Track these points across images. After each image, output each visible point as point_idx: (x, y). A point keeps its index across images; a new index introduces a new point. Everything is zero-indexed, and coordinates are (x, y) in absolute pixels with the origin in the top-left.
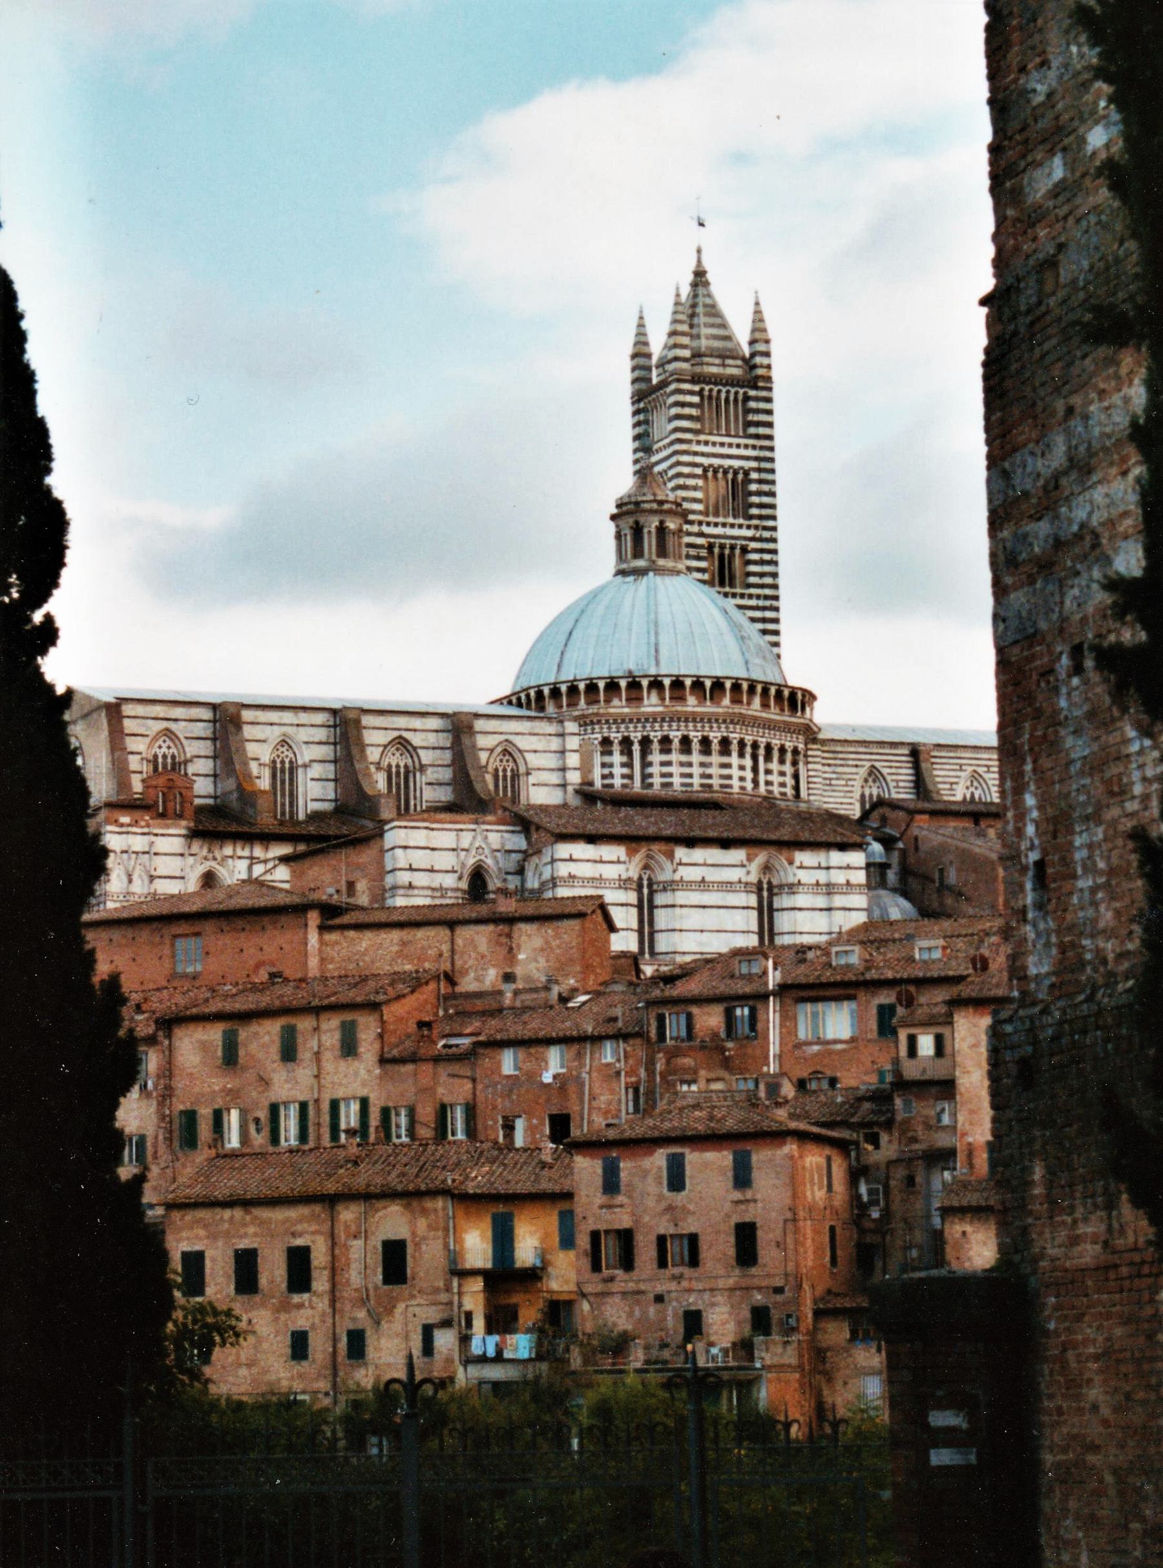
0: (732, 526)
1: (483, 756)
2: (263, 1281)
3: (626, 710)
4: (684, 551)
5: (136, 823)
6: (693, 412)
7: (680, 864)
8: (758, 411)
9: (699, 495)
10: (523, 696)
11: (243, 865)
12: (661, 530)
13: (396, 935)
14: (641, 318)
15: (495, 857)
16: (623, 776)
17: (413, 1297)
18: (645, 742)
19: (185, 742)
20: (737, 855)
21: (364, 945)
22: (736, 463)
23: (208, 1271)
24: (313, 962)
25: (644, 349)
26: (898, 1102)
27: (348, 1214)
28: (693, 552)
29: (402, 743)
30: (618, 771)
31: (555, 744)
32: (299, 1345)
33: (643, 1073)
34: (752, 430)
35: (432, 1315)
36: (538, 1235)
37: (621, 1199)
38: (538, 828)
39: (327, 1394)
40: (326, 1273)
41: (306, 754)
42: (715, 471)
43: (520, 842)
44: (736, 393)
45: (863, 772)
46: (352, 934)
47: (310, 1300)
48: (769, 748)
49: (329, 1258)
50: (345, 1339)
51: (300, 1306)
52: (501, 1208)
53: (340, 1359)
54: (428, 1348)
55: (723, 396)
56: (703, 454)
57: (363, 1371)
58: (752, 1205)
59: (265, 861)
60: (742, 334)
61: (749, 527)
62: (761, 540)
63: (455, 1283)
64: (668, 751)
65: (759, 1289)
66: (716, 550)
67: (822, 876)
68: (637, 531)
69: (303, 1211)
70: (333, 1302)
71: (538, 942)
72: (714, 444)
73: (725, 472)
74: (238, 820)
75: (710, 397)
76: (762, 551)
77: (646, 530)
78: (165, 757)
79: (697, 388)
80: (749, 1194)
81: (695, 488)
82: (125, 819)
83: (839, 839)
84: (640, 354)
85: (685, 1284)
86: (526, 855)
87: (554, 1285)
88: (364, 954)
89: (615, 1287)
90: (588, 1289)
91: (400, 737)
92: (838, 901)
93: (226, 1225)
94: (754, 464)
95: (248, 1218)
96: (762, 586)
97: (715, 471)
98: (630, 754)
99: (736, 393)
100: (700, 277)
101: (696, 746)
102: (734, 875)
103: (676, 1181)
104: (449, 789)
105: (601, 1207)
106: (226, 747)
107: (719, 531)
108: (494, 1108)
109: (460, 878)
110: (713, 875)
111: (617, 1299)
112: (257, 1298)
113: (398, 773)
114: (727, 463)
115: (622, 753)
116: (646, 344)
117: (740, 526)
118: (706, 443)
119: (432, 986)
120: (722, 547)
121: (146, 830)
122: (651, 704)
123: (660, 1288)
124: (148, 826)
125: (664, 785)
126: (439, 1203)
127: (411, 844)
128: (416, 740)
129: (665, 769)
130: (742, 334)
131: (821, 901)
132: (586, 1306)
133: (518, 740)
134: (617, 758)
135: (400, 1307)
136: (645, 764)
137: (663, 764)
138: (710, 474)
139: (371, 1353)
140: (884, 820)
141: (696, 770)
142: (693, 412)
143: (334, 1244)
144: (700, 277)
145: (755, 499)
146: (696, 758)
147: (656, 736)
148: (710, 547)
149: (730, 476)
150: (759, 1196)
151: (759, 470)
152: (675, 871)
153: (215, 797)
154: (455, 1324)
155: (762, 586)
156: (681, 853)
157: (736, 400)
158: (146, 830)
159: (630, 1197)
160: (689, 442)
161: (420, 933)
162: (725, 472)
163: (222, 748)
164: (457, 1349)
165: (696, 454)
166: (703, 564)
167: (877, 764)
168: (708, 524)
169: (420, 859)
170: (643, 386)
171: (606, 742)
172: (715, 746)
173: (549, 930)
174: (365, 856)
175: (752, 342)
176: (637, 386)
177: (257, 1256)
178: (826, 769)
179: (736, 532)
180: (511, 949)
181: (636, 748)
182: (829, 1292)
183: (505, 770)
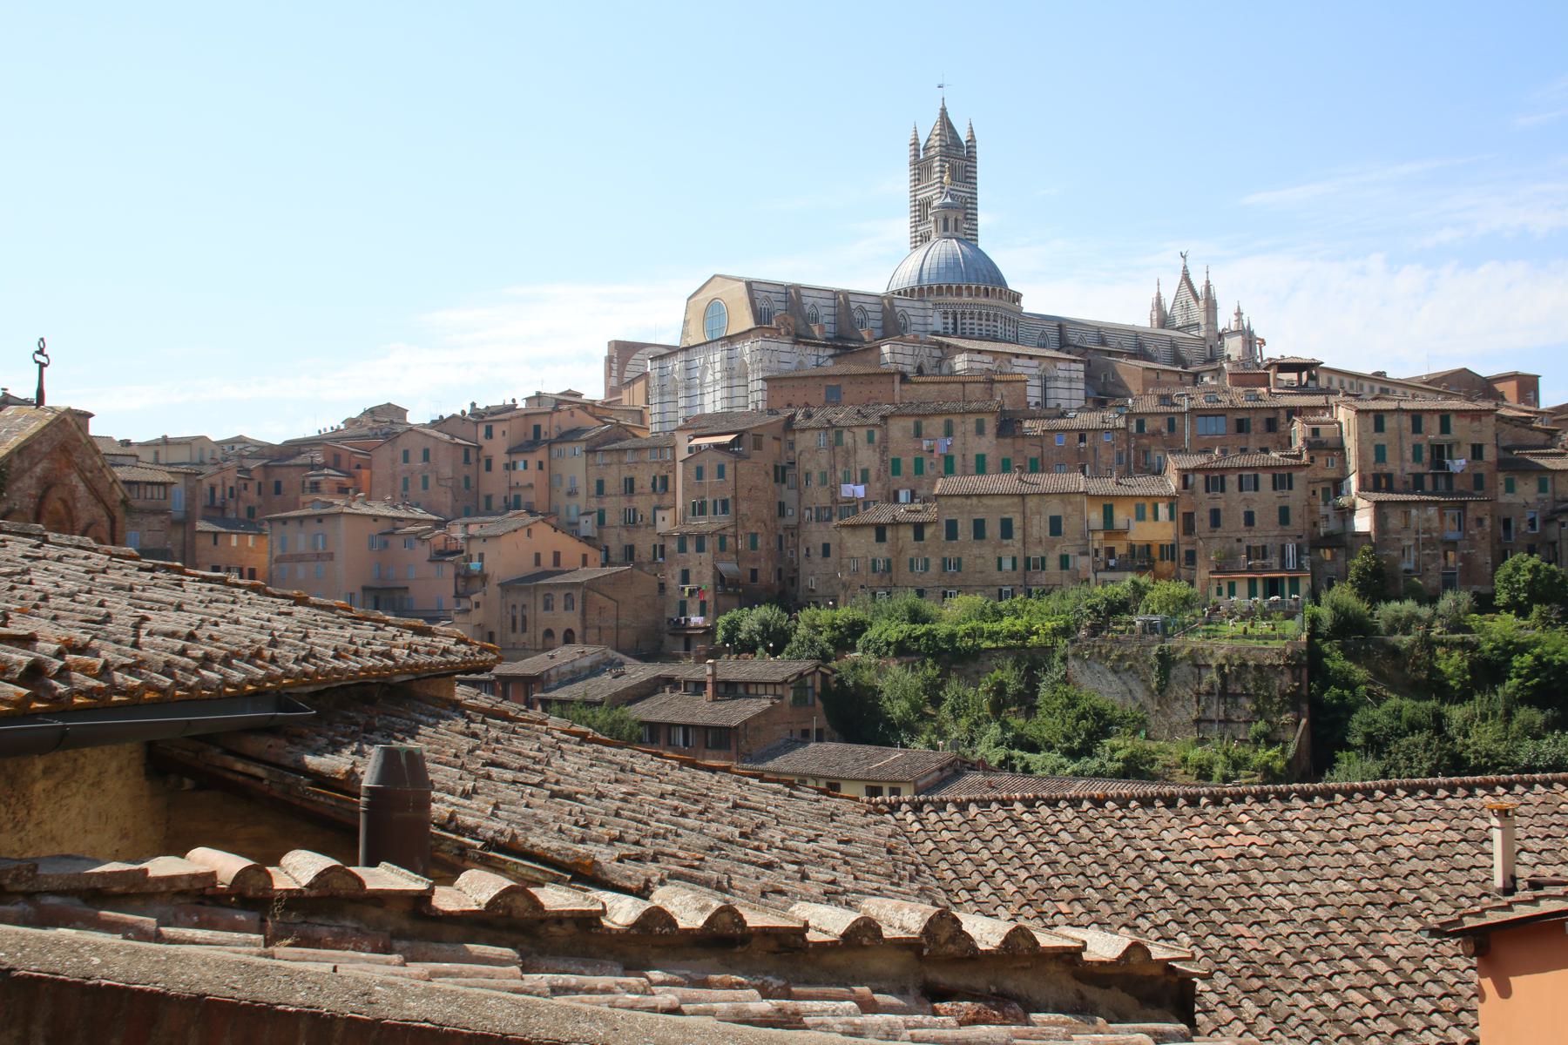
2: (988, 534)
13: (936, 387)
18: (963, 313)
20: (1035, 363)
24: (897, 399)
29: (861, 309)
31: (922, 313)
33: (1125, 446)
40: (1020, 531)
41: (823, 311)
43: (937, 353)
51: (1007, 545)
60: (964, 137)
67: (1067, 374)
68: (946, 220)
69: (1009, 501)
70: (1024, 543)
84: (916, 143)
92: (1074, 385)
100: (944, 112)
101: (984, 317)
102: (1034, 371)
112: (985, 541)
122: (965, 299)
123: (1239, 536)
126: (1078, 498)
128: (867, 307)
131: (1066, 385)
134: (950, 321)
135: (1058, 546)
141: (983, 327)
144: (944, 112)
146: (984, 322)
156: (1014, 360)
161: (948, 387)
171: (946, 313)
172: (992, 318)
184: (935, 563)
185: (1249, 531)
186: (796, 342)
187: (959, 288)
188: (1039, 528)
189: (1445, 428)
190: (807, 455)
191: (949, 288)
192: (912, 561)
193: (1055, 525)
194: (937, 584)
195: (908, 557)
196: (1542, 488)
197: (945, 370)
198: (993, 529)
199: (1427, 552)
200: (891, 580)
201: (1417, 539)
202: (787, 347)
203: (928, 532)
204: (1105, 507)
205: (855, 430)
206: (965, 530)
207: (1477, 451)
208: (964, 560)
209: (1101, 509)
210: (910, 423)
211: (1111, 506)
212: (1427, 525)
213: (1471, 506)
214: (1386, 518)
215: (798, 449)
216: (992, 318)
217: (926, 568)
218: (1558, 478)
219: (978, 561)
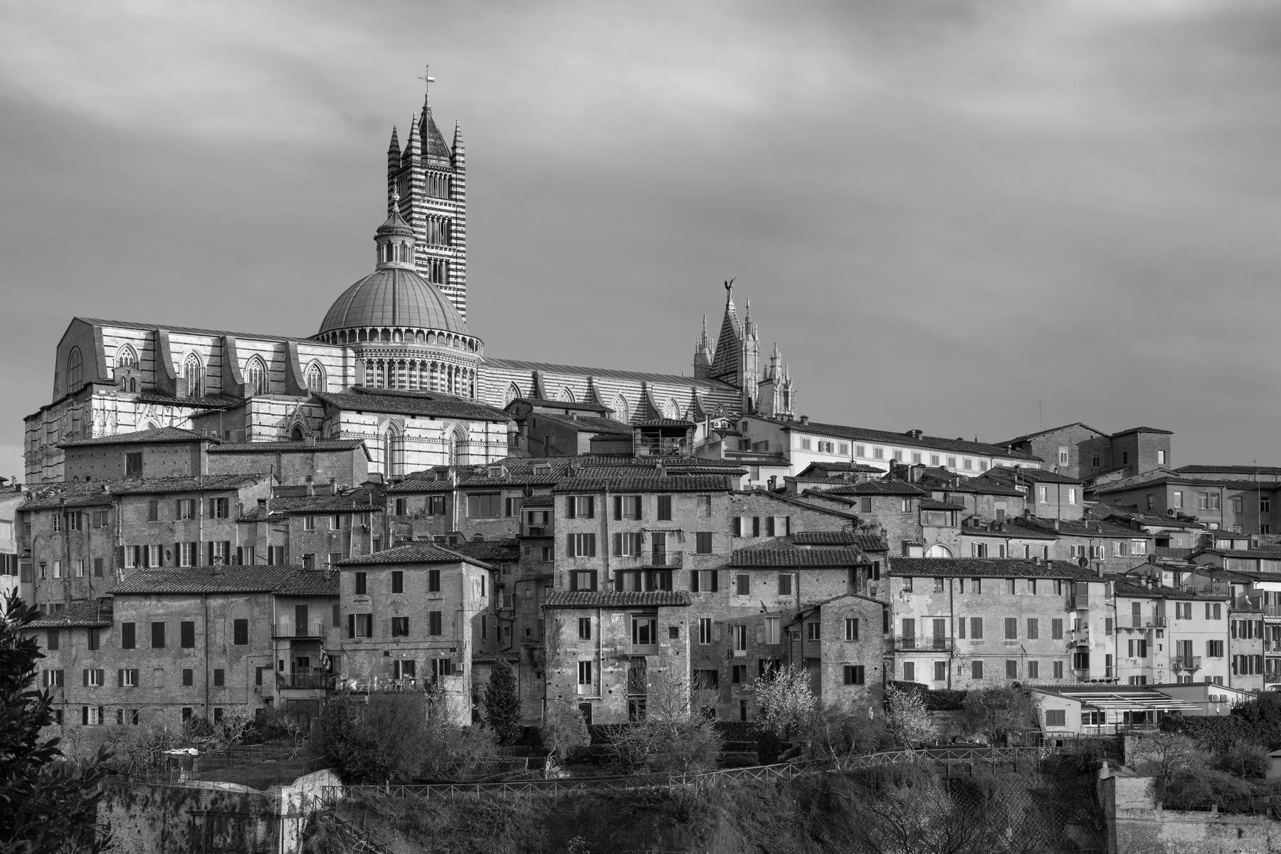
0: (441, 249)
1: (302, 367)
2: (167, 641)
3: (381, 345)
4: (415, 261)
5: (109, 394)
6: (422, 184)
7: (407, 427)
8: (456, 186)
9: (424, 230)
10: (325, 335)
11: (167, 420)
12: (404, 246)
14: (395, 132)
15: (307, 421)
16: (378, 381)
17: (251, 651)
19: (137, 351)
20: (438, 423)
21: (232, 462)
22: (444, 214)
23: (137, 633)
25: (396, 149)
26: (522, 548)
27: (215, 603)
28: (419, 262)
30: (376, 378)
32: (188, 678)
34: (454, 196)
35: (262, 662)
36: (321, 619)
37: (367, 597)
38: (331, 405)
39: (203, 705)
40: (203, 637)
42: (433, 218)
43: (318, 412)
44: (445, 175)
45: (508, 385)
46: (226, 456)
47: (194, 652)
48: (457, 370)
49: (205, 629)
50: (213, 674)
51: (189, 655)
52: (301, 603)
53: (210, 686)
54: (259, 680)
55: (438, 176)
56: (426, 208)
57: (223, 692)
58: (440, 601)
59: (180, 418)
60: (449, 145)
61: (450, 250)
62: (456, 257)
63: (274, 644)
64: (404, 368)
65: (442, 649)
66: (432, 262)
70: (207, 653)
71: (327, 463)
72: (433, 202)
73: (438, 219)
74: (165, 394)
75: (431, 176)
76: (457, 264)
77: (394, 246)
78: (126, 359)
79: (424, 171)
80: (438, 595)
81: (422, 227)
82: (103, 392)
83: (494, 418)
85: (401, 646)
86: (324, 420)
87: (330, 647)
88: (232, 467)
89: (361, 647)
90: (347, 647)
91: (257, 354)
93: (147, 608)
94: (454, 215)
95: (159, 604)
96: (457, 283)
97: (433, 218)
98: (383, 369)
99: (445, 175)
102: (437, 434)
103: (397, 586)
104: (283, 384)
105: (355, 601)
106: (160, 355)
107: (434, 251)
108: (300, 549)
109: (287, 431)
110: (424, 434)
111: (363, 653)
112: (164, 650)
113: (256, 375)
114: (440, 213)
115: (378, 368)
116: (398, 147)
117: (446, 249)
118: (428, 202)
119: (267, 481)
120: (436, 260)
121: (114, 398)
122: (396, 342)
123: (387, 648)
124: (115, 396)
125: (400, 387)
127: (261, 411)
129: (401, 378)
130: (449, 145)
132: (345, 658)
133: (321, 359)
135: (244, 657)
136: (390, 376)
137: (400, 375)
138: (430, 219)
139: (227, 683)
140: (518, 410)
142: (422, 184)
143: (207, 621)
145: (454, 235)
147: (396, 360)
148: (429, 260)
149: (441, 221)
150: (443, 597)
151: (457, 218)
152: (404, 431)
153: (154, 383)
154: (274, 667)
155: (457, 283)
156: (408, 421)
157: (445, 179)
158: (114, 398)
159: (372, 596)
160: (419, 200)
162: (438, 219)
163: (158, 356)
164: (275, 681)
165: (422, 207)
166: (425, 269)
167: (515, 381)
168: (428, 247)
169: (264, 419)
170: (395, 169)
173: (334, 456)
174: (236, 417)
175: (454, 148)
176: (392, 169)
177: (164, 626)
178: (488, 382)
179: (443, 252)
180: (313, 466)
181: (386, 366)
182: (481, 652)
183: (314, 375)
184: (110, 675)
185: (397, 642)
186: (139, 401)
187: (386, 332)
188: (223, 634)
189: (664, 513)
190: (41, 542)
191: (374, 332)
192: (86, 672)
193: (241, 631)
194: (112, 701)
195: (83, 668)
196: (784, 588)
197: (327, 435)
198: (173, 635)
199: (610, 669)
200: (63, 695)
201: (598, 654)
202: (131, 407)
203: (104, 638)
204: (298, 608)
205: (90, 511)
206: (143, 636)
207: (704, 543)
208: (141, 672)
209: (293, 611)
210: (144, 505)
211: (306, 607)
212: (610, 636)
213: (662, 612)
214: (559, 627)
215: (33, 534)
216: (429, 367)
217: (101, 682)
218: (804, 574)
219: (157, 674)
